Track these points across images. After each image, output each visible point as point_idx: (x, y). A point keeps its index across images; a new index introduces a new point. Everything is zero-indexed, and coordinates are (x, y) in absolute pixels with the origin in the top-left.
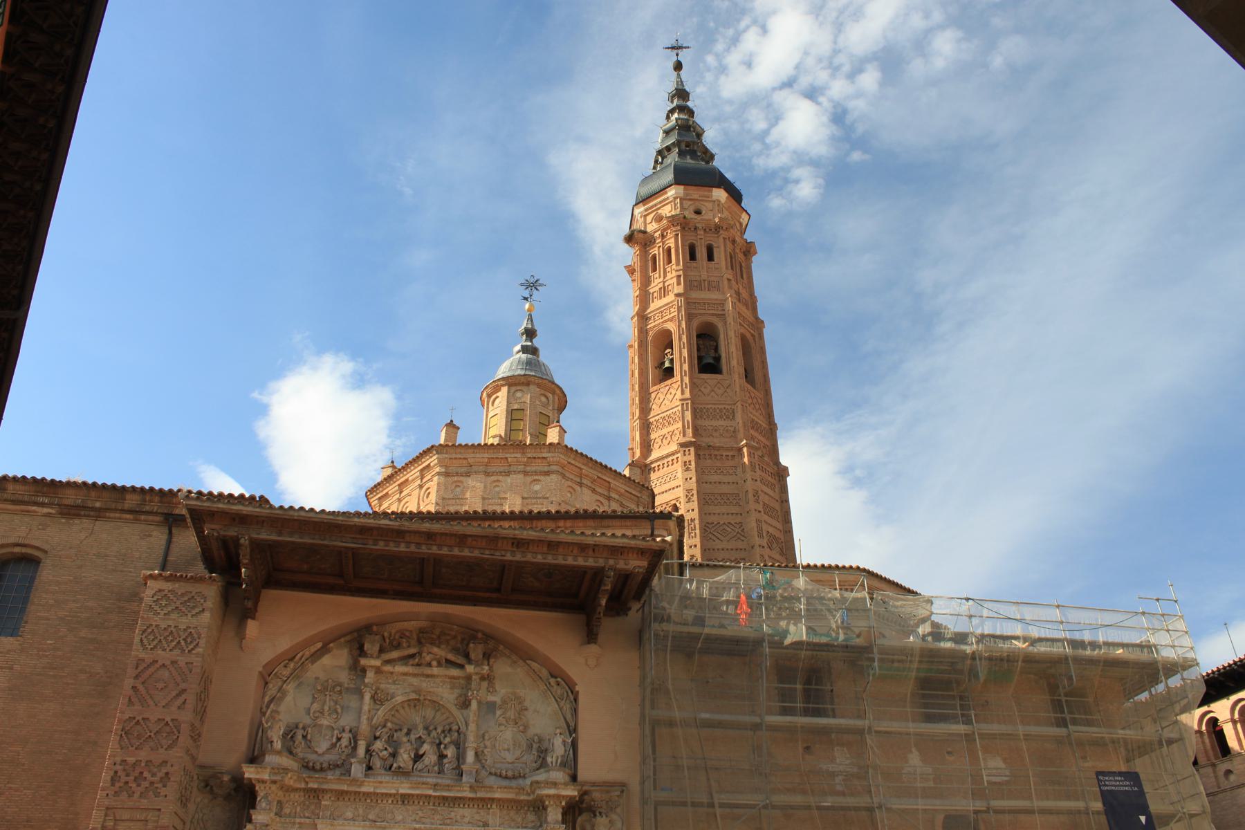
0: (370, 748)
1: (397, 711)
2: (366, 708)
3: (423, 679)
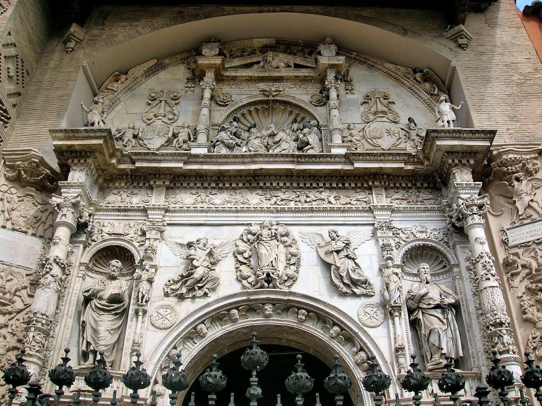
1: (243, 115)
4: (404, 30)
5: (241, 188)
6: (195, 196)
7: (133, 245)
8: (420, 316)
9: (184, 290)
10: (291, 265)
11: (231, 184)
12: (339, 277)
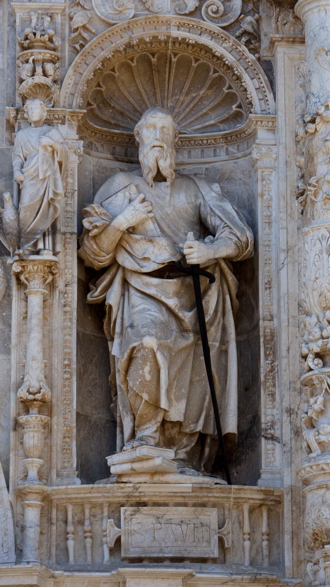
8: (113, 298)
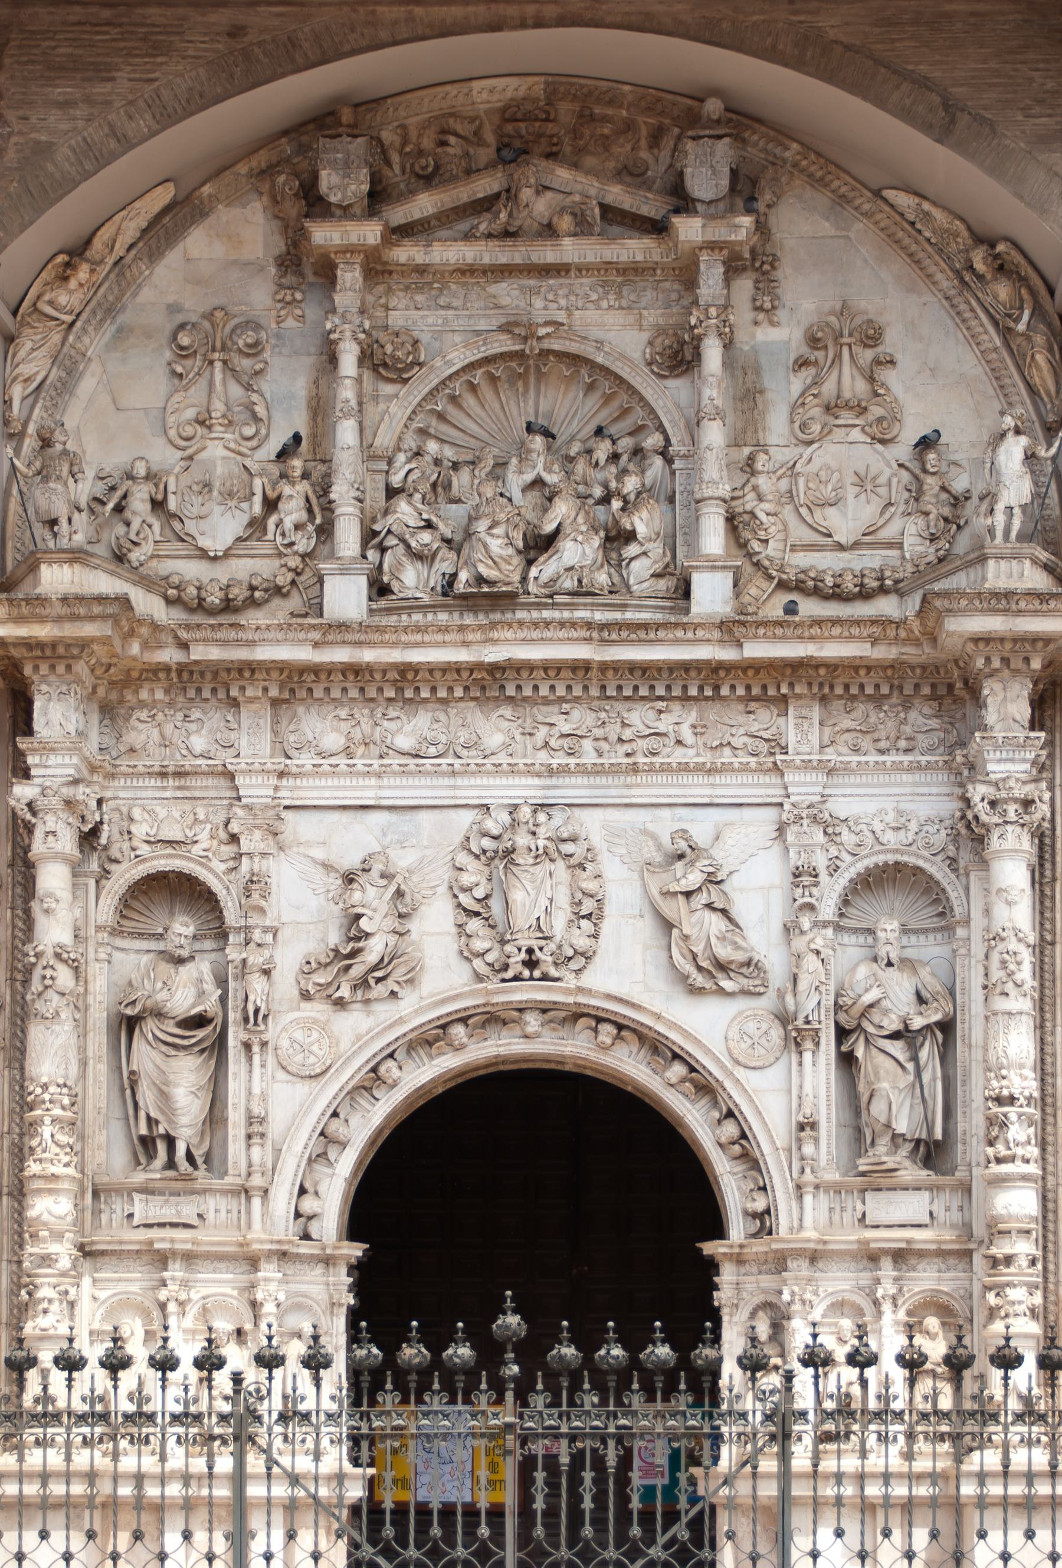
0: (377, 527)
1: (454, 399)
2: (347, 393)
3: (532, 282)
4: (946, 106)
5: (461, 699)
6: (345, 726)
7: (211, 870)
8: (860, 1053)
9: (345, 992)
10: (583, 917)
11: (434, 690)
12: (690, 956)
